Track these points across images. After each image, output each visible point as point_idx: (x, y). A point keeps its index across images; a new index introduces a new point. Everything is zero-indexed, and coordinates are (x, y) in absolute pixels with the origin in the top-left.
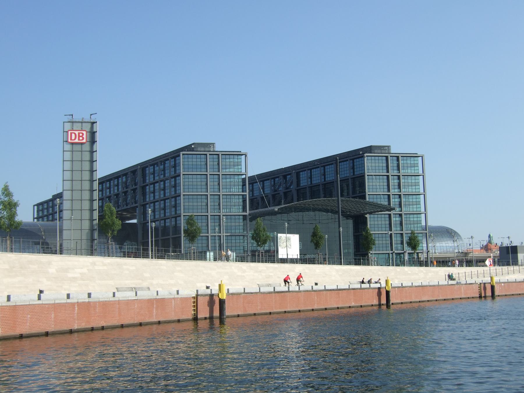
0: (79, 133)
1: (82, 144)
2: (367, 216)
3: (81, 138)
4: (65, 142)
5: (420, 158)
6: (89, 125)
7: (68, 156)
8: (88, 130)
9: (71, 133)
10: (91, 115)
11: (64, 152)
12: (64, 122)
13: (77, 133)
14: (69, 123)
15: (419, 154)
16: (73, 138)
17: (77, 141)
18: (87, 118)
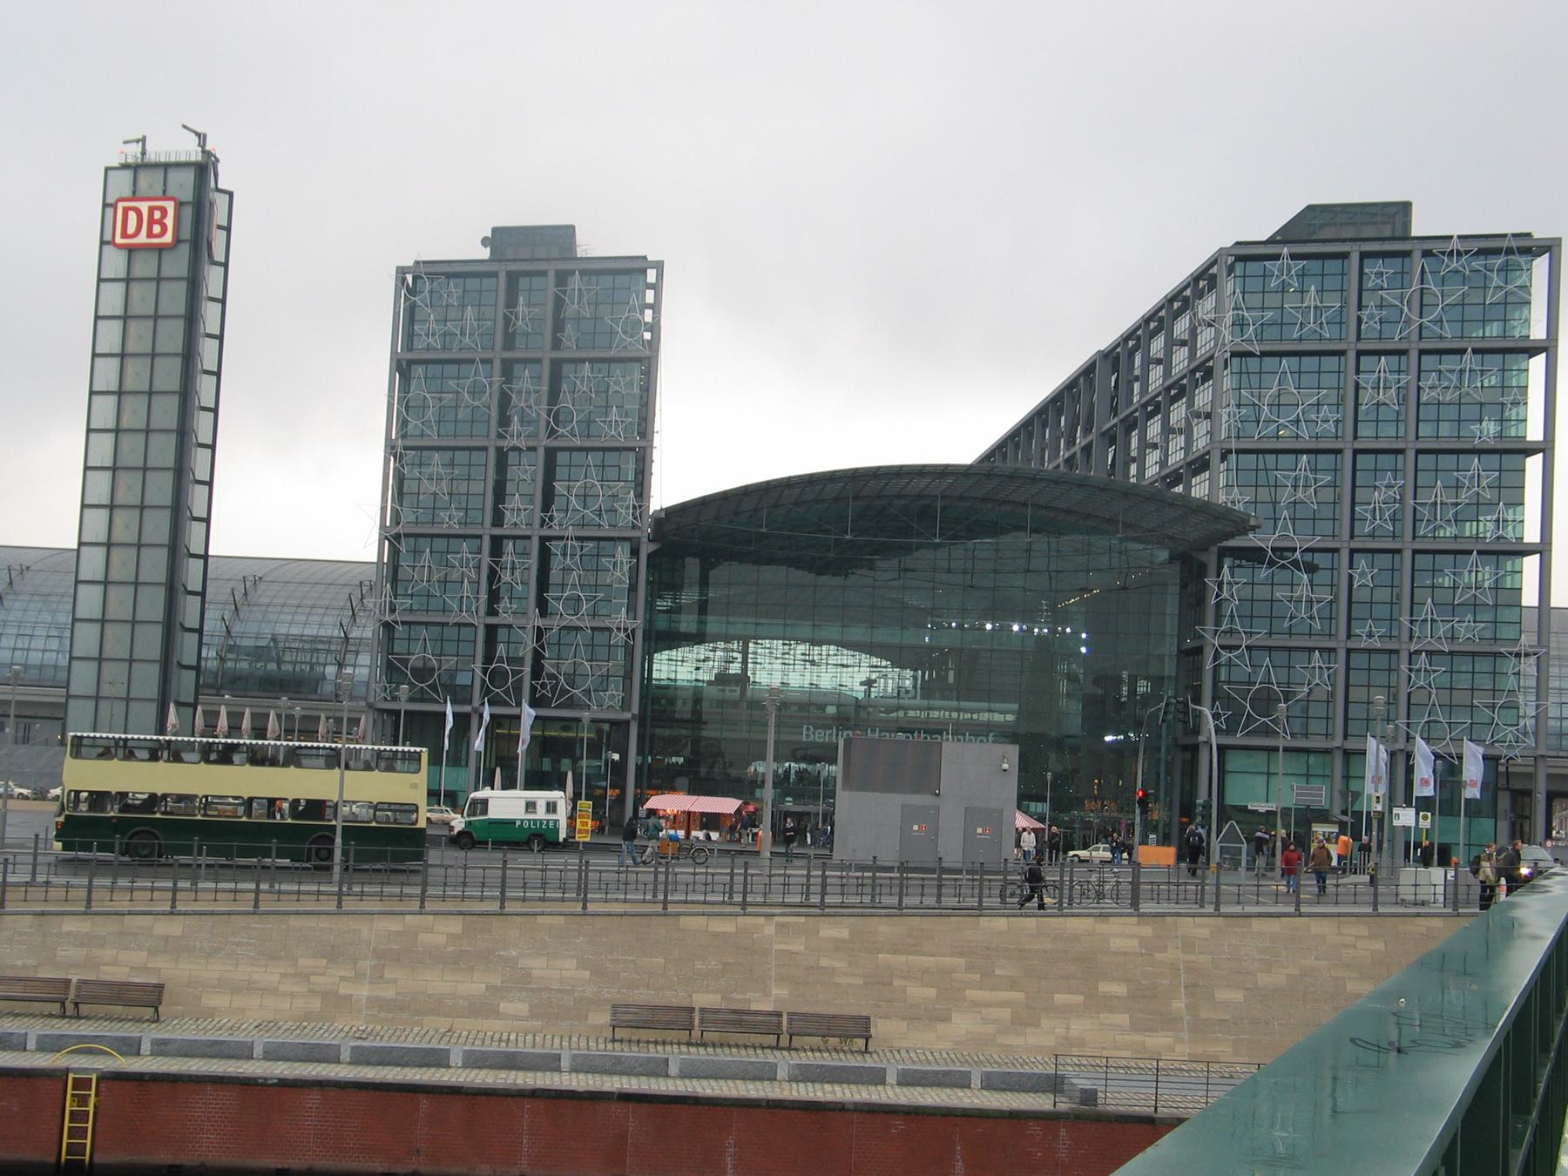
0: (152, 210)
1: (161, 249)
2: (1211, 559)
3: (157, 229)
4: (106, 248)
5: (1541, 265)
6: (189, 177)
7: (115, 294)
8: (187, 194)
9: (126, 211)
11: (102, 285)
12: (107, 169)
13: (144, 207)
14: (128, 174)
15: (1540, 233)
16: (131, 229)
17: (142, 238)
18: (188, 150)
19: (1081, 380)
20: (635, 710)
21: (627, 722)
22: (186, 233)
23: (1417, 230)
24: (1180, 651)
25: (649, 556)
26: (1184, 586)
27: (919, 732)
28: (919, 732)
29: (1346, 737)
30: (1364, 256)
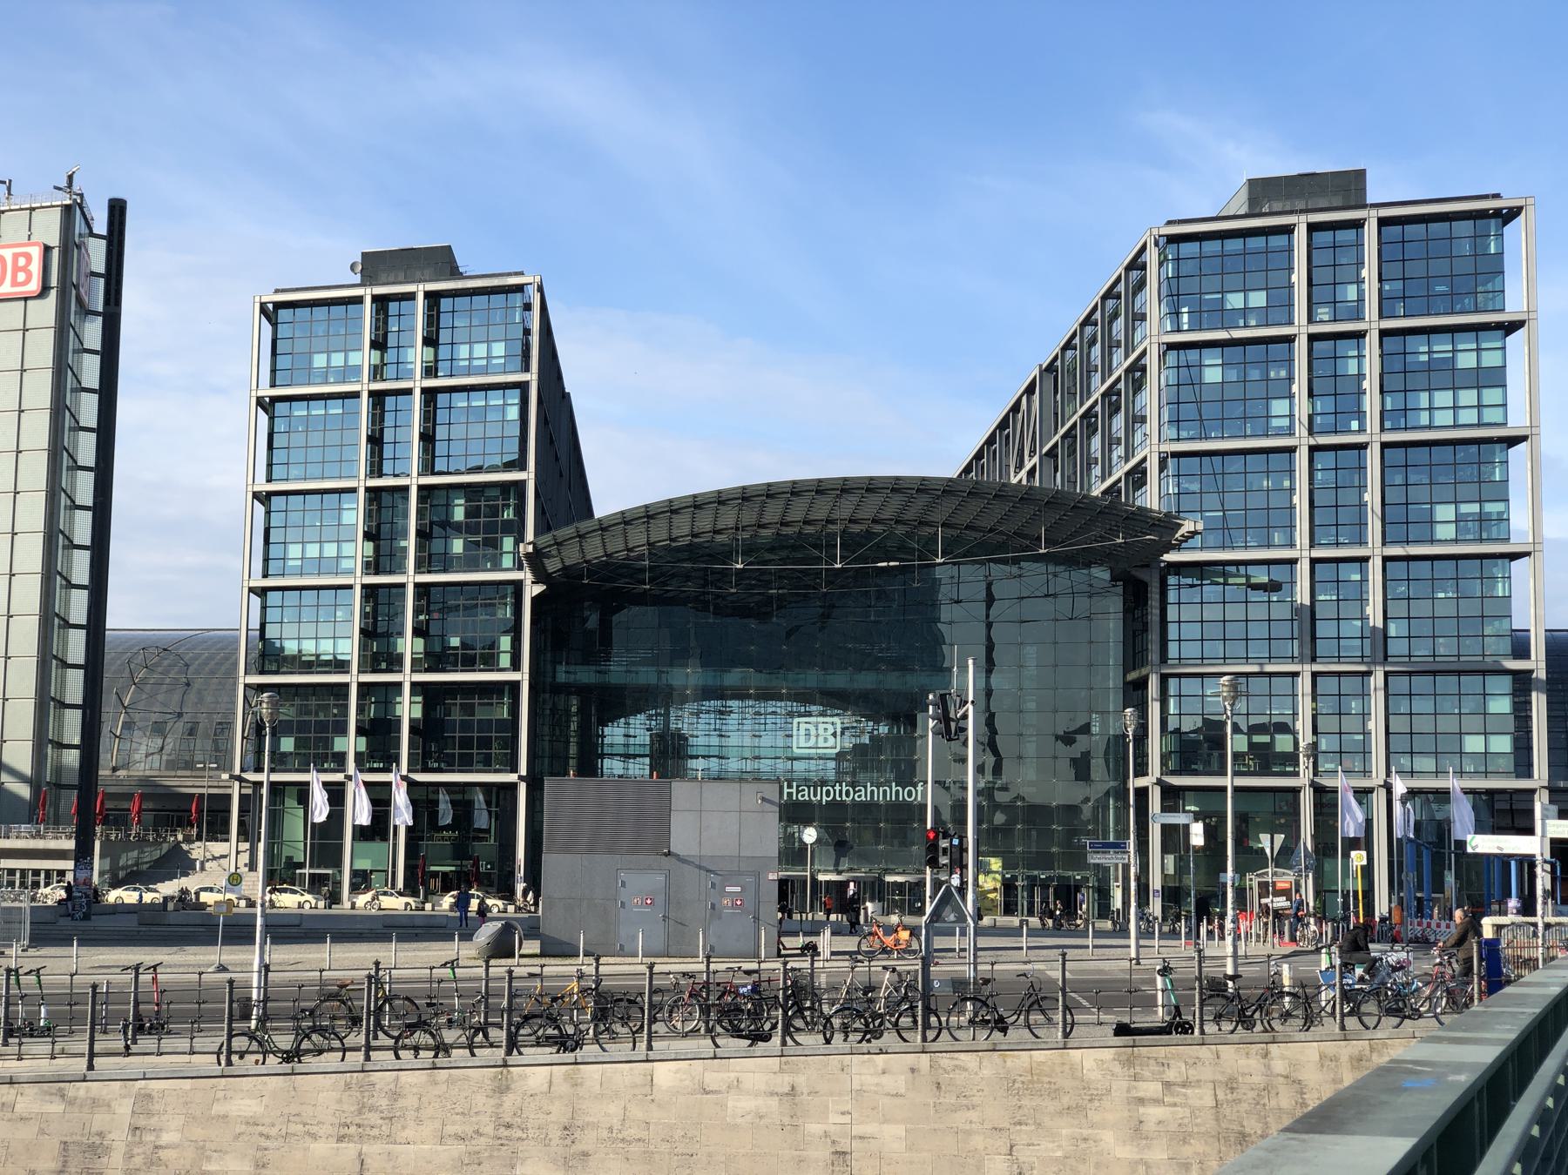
0: (16, 257)
1: (26, 299)
3: (21, 277)
6: (56, 215)
8: (54, 240)
10: (70, 178)
19: (1024, 399)
20: (524, 772)
21: (512, 787)
22: (54, 281)
23: (1369, 201)
24: (1126, 684)
25: (532, 598)
26: (1125, 611)
27: (841, 786)
28: (841, 786)
29: (1315, 774)
30: (1312, 228)
